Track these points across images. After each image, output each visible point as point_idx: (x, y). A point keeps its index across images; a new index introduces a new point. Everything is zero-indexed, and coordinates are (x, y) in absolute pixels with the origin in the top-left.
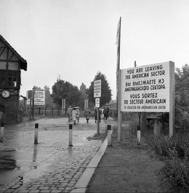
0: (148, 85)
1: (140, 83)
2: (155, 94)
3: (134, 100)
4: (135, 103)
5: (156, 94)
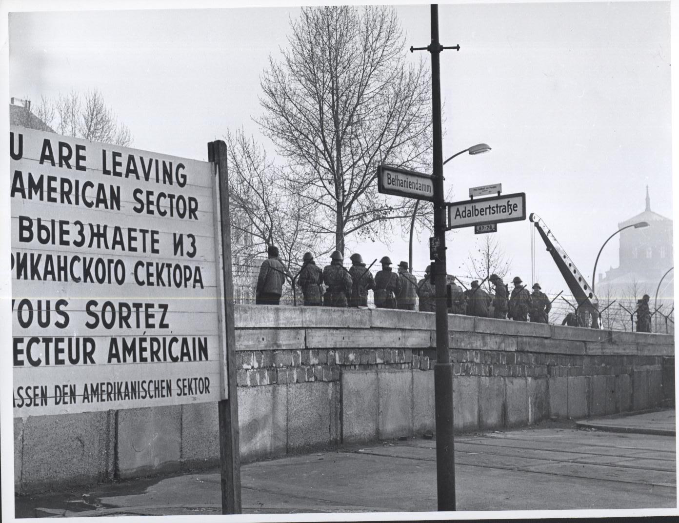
0: (118, 253)
1: (67, 233)
2: (161, 306)
3: (26, 341)
4: (37, 364)
5: (164, 307)
